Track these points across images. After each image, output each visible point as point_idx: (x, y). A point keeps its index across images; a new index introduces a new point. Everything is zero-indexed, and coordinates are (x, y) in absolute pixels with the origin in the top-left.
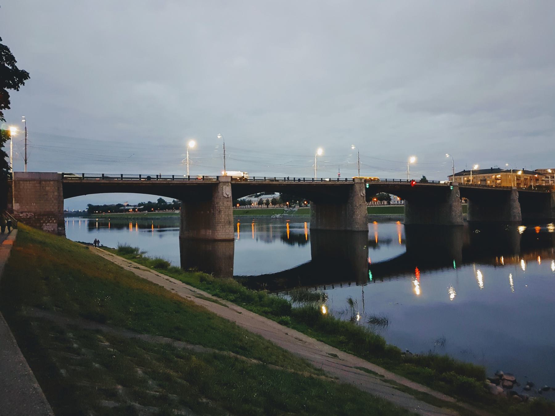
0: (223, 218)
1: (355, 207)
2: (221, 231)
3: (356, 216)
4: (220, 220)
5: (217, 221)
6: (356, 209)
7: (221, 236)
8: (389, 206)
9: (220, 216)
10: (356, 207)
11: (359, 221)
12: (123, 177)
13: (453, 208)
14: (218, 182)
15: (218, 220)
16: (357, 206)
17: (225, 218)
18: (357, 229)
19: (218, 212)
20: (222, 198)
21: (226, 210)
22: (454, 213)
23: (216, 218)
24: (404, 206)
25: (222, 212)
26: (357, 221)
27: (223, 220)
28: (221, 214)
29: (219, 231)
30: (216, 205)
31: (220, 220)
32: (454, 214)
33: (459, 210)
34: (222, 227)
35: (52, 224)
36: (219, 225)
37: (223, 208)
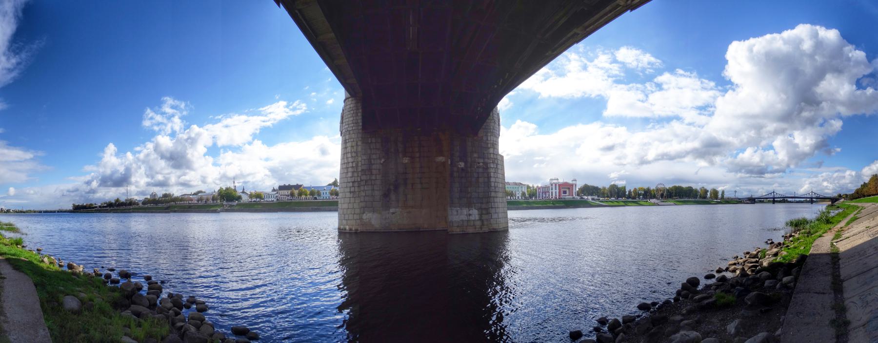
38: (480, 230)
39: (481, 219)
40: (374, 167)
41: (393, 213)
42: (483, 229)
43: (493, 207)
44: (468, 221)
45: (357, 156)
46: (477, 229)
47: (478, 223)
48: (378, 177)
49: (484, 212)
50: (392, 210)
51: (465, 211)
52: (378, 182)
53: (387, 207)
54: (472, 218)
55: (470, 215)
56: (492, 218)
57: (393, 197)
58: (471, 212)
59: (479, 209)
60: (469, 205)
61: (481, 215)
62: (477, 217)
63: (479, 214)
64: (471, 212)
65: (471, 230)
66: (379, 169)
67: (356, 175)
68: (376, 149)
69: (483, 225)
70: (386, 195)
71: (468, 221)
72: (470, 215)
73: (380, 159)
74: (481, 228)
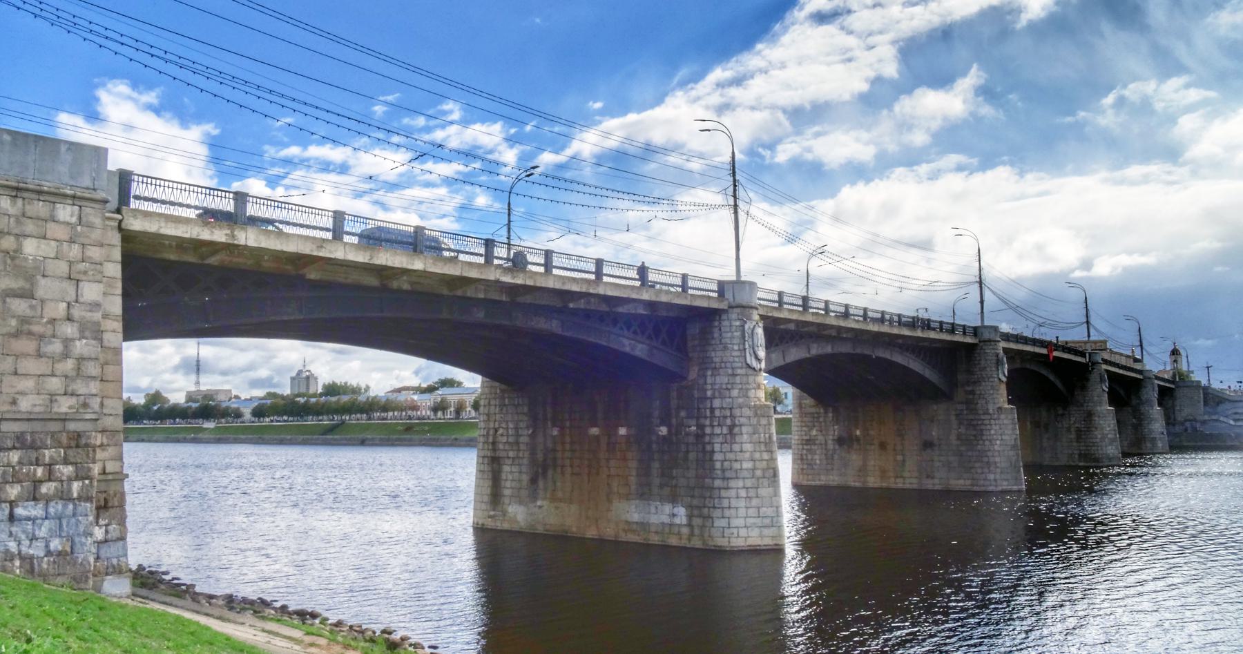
0: (747, 455)
1: (983, 417)
2: (742, 512)
3: (987, 443)
4: (737, 466)
5: (723, 470)
6: (987, 422)
7: (743, 532)
8: (457, 421)
9: (736, 447)
10: (988, 417)
11: (997, 459)
12: (505, 256)
13: (1096, 418)
14: (723, 306)
15: (726, 464)
16: (991, 411)
17: (757, 456)
18: (994, 483)
19: (725, 430)
20: (739, 371)
21: (759, 421)
22: (1098, 434)
23: (718, 456)
24: (791, 416)
25: (744, 429)
26: (992, 460)
27: (747, 465)
28: (738, 439)
29: (733, 512)
30: (717, 403)
31: (737, 466)
32: (1099, 436)
33: (1109, 426)
34: (743, 493)
35: (56, 507)
36: (732, 484)
37: (747, 412)
38: (687, 542)
39: (690, 525)
40: (522, 439)
41: (540, 507)
42: (692, 543)
43: (716, 505)
44: (671, 525)
45: (489, 420)
46: (683, 542)
47: (685, 531)
48: (527, 454)
49: (696, 512)
50: (539, 503)
51: (667, 508)
52: (525, 461)
53: (534, 497)
54: (677, 521)
55: (674, 515)
56: (713, 526)
57: (541, 483)
58: (676, 510)
59: (689, 507)
60: (674, 499)
61: (690, 517)
62: (685, 521)
63: (687, 516)
64: (676, 510)
65: (673, 541)
66: (527, 444)
67: (486, 447)
68: (524, 414)
69: (692, 534)
70: (534, 481)
71: (671, 525)
72: (674, 515)
73: (528, 428)
74: (689, 540)
